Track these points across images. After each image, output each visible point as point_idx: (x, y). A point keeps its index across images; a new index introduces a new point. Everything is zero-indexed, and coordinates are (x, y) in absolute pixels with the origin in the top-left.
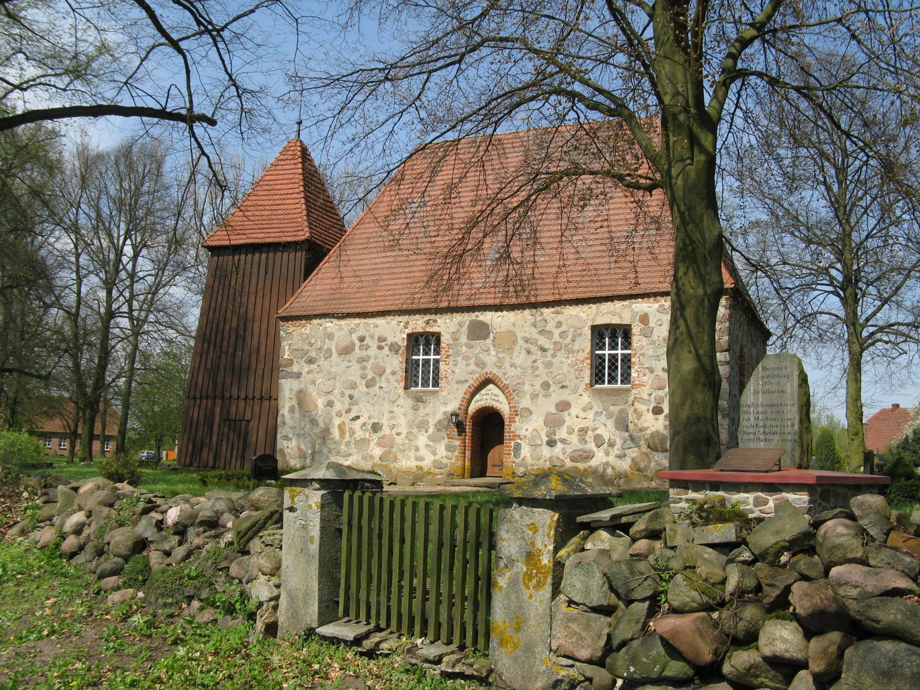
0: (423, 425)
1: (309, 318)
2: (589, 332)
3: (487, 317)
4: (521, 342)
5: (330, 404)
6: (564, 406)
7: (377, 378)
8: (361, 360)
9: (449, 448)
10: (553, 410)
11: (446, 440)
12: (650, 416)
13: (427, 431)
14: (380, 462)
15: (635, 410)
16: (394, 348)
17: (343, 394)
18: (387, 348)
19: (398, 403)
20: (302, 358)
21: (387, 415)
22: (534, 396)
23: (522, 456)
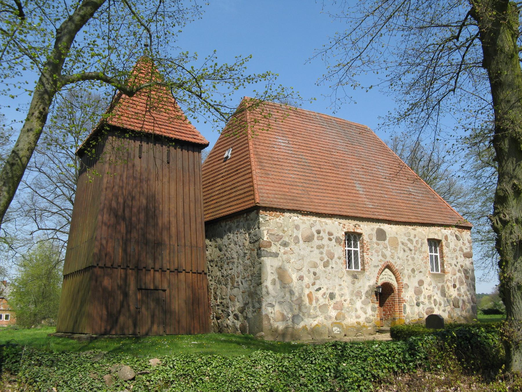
0: (358, 294)
1: (283, 211)
2: (427, 242)
3: (385, 227)
4: (400, 244)
5: (301, 278)
6: (421, 283)
7: (330, 260)
8: (319, 247)
9: (373, 309)
10: (417, 286)
11: (371, 304)
12: (452, 289)
13: (361, 299)
14: (335, 321)
15: (447, 286)
16: (338, 240)
17: (309, 271)
18: (334, 240)
19: (343, 279)
20: (278, 241)
21: (338, 287)
22: (409, 277)
23: (407, 312)
